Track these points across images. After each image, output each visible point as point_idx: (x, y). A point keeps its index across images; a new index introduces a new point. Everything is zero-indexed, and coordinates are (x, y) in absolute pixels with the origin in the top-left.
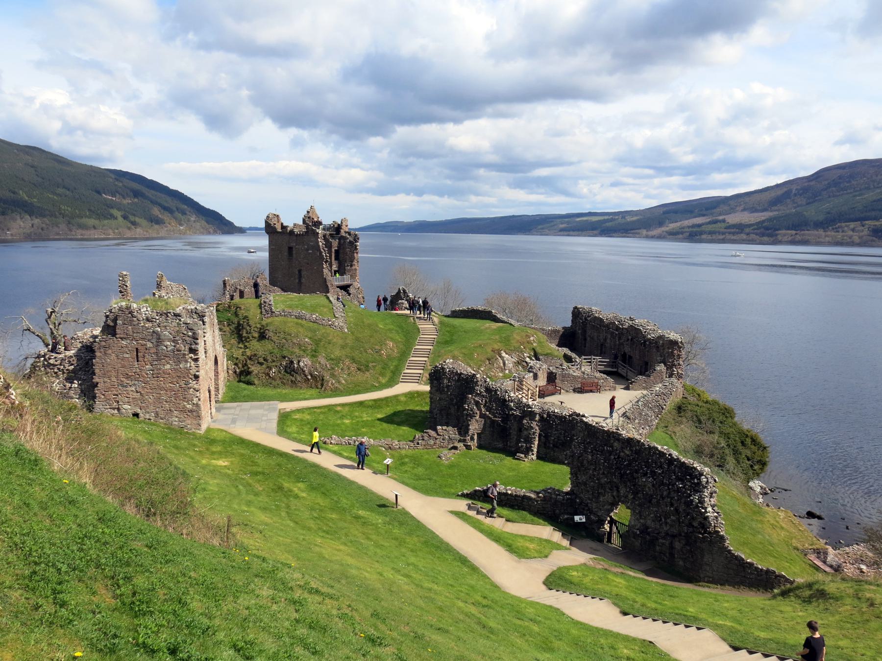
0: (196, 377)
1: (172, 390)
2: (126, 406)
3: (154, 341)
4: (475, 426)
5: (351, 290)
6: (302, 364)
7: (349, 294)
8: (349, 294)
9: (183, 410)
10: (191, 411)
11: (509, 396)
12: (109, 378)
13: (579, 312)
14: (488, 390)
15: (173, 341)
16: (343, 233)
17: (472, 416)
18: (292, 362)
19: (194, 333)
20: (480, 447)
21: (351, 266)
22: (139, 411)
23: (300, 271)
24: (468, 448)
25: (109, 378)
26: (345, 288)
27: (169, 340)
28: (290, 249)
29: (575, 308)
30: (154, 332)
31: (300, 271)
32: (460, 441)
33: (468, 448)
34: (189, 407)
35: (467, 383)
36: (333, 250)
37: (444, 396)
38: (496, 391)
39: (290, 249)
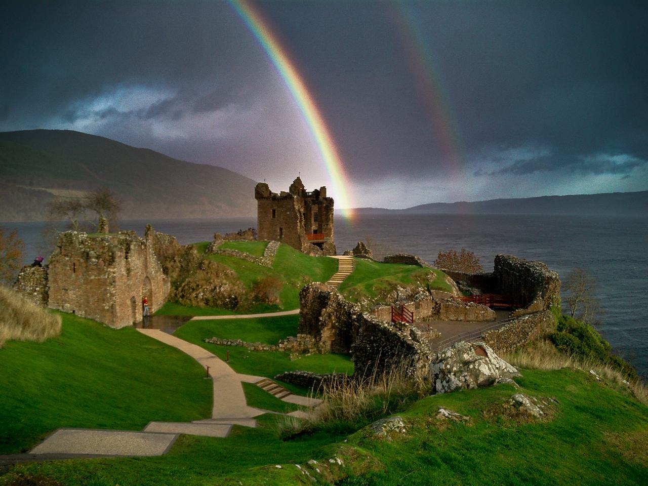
5: (324, 246)
6: (222, 289)
8: (322, 249)
9: (103, 310)
10: (108, 310)
11: (354, 310)
13: (500, 261)
16: (321, 197)
17: (324, 325)
19: (113, 254)
20: (333, 352)
21: (327, 225)
23: (281, 229)
28: (274, 211)
29: (497, 256)
30: (84, 252)
34: (107, 308)
35: (323, 299)
36: (313, 212)
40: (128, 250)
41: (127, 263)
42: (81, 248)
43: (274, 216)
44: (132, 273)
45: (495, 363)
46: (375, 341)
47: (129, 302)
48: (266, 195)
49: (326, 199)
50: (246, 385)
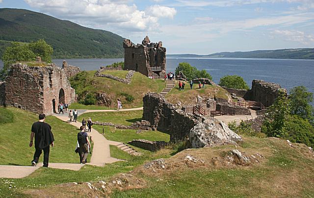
0: (42, 93)
1: (32, 98)
2: (16, 103)
3: (26, 78)
4: (157, 121)
5: (160, 73)
7: (159, 75)
8: (159, 75)
9: (37, 106)
12: (10, 92)
14: (164, 104)
15: (33, 78)
17: (156, 116)
18: (99, 95)
19: (42, 76)
22: (20, 105)
23: (137, 64)
24: (153, 130)
25: (10, 92)
26: (158, 73)
27: (32, 78)
28: (133, 54)
31: (137, 64)
32: (150, 127)
33: (153, 130)
37: (148, 108)
38: (167, 105)
39: (133, 54)
40: (50, 74)
41: (51, 81)
42: (24, 73)
43: (133, 57)
44: (52, 86)
45: (228, 132)
46: (181, 124)
47: (52, 102)
48: (129, 45)
49: (162, 48)
50: (111, 146)
